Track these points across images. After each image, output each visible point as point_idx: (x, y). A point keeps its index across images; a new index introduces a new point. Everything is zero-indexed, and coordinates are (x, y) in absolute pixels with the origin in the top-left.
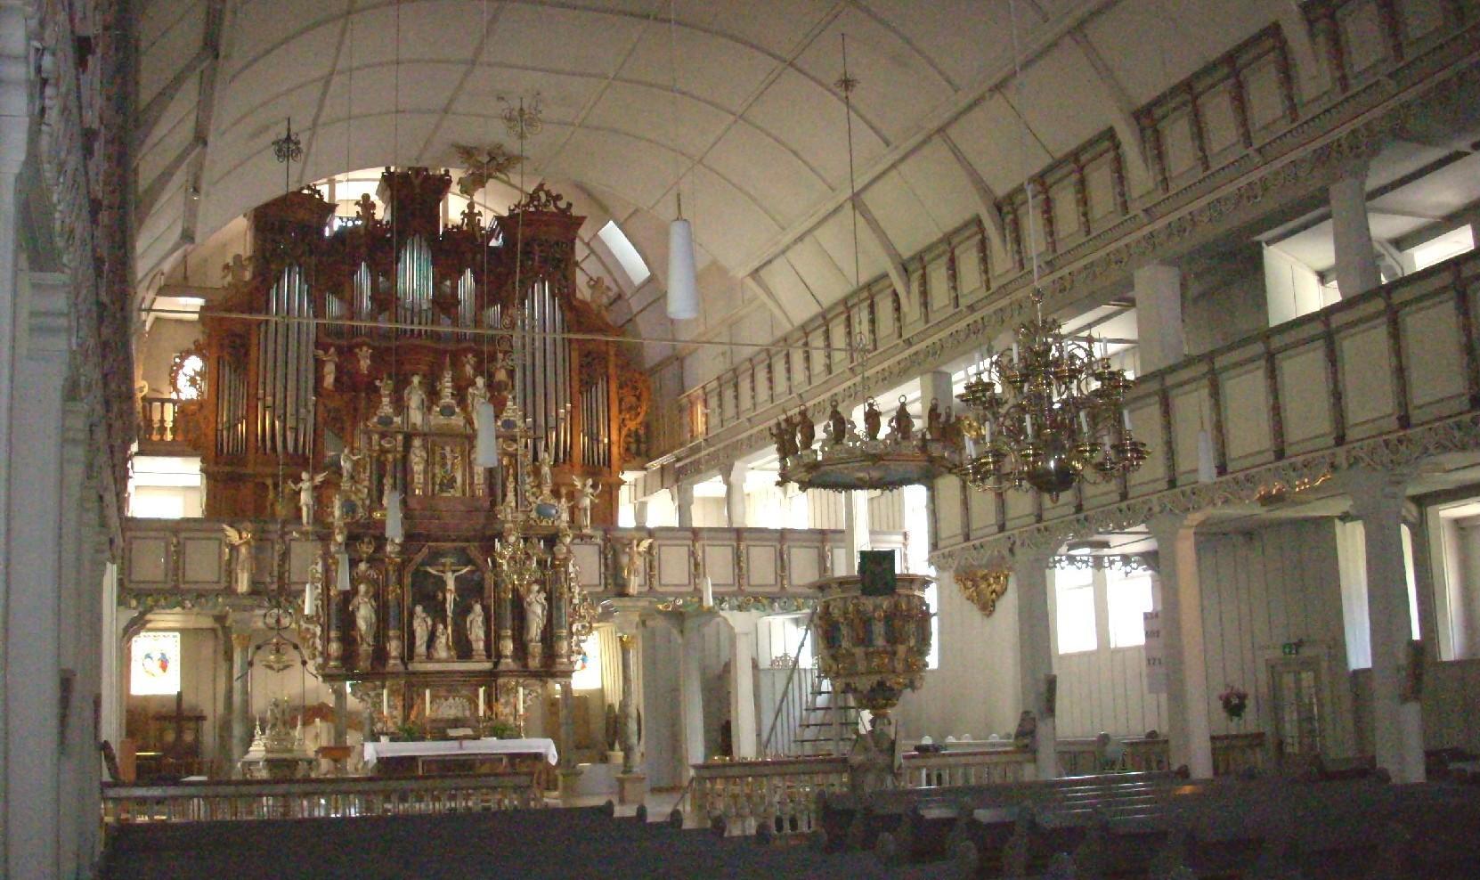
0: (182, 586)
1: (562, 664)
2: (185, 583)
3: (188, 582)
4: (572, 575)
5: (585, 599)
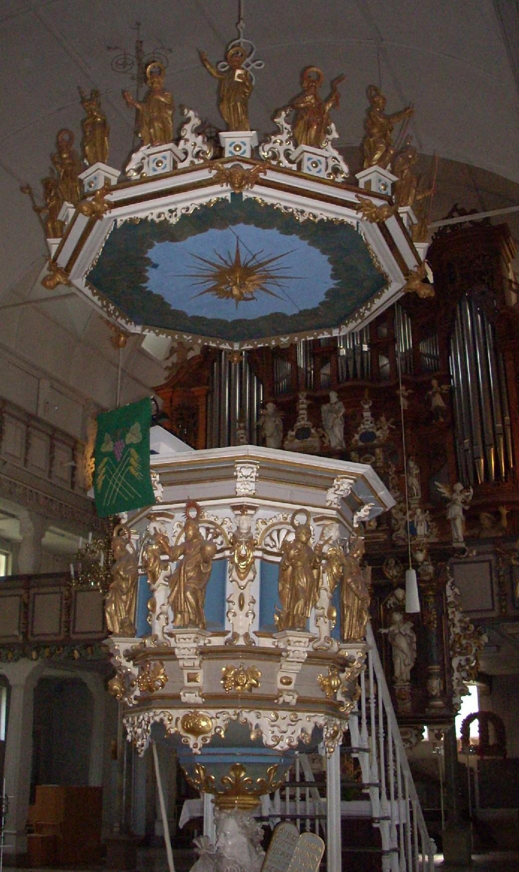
0: (74, 637)
1: (434, 707)
2: (74, 632)
3: (77, 633)
4: (450, 599)
5: (464, 629)
